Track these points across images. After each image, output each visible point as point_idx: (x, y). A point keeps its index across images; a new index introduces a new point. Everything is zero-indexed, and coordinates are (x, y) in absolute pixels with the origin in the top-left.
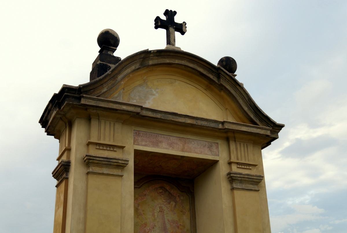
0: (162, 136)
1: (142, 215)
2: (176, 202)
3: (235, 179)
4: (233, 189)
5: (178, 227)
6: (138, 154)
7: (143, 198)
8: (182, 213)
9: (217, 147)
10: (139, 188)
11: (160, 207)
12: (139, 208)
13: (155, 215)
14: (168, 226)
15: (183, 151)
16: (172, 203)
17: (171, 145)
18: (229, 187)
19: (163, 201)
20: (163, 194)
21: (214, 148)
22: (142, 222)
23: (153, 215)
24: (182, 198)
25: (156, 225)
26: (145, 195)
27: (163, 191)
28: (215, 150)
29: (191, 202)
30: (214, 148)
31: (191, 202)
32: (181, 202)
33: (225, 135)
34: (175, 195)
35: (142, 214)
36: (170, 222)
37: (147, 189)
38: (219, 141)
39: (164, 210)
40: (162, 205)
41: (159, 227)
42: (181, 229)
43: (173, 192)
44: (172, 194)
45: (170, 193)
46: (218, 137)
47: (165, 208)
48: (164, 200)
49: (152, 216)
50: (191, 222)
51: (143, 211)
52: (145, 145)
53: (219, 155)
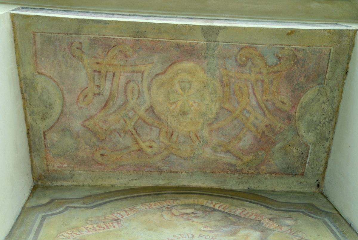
2: (264, 230)
10: (92, 207)
19: (202, 229)
24: (289, 222)
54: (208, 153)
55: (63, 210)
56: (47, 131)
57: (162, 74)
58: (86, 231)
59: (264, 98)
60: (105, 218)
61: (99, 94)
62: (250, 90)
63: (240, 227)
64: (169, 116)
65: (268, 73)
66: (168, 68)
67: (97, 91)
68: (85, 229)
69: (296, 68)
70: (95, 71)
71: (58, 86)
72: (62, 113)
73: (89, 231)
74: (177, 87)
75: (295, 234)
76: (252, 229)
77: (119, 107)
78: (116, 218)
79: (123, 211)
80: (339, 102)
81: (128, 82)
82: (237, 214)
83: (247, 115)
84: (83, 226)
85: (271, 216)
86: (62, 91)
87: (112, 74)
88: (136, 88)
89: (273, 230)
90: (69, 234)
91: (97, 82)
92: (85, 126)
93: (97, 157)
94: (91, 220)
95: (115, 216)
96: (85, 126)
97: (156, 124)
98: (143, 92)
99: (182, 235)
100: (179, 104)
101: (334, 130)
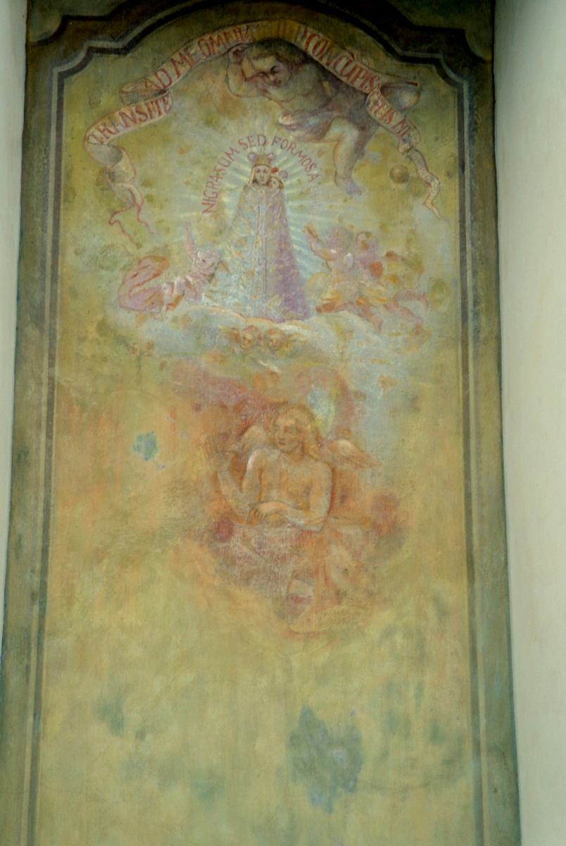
1: (139, 210)
2: (365, 127)
5: (376, 270)
7: (145, 110)
8: (402, 186)
11: (256, 161)
12: (123, 166)
13: (222, 206)
14: (308, 266)
16: (335, 131)
19: (281, 121)
20: (277, 84)
22: (139, 246)
23: (212, 204)
24: (407, 99)
25: (228, 259)
26: (162, 92)
27: (282, 66)
32: (403, 122)
34: (357, 84)
35: (139, 200)
36: (319, 241)
37: (177, 57)
39: (286, 175)
40: (269, 148)
41: (250, 274)
42: (394, 278)
43: (347, 65)
44: (344, 79)
45: (322, 70)
47: (291, 163)
48: (285, 114)
49: (205, 211)
50: (463, 235)
51: (147, 183)
55: (84, 59)
60: (146, 86)
63: (335, 114)
68: (120, 119)
73: (127, 126)
75: (406, 136)
78: (162, 87)
79: (171, 63)
82: (336, 72)
84: (117, 110)
85: (385, 79)
89: (379, 124)
90: (100, 130)
94: (126, 90)
95: (160, 80)
99: (251, 139)
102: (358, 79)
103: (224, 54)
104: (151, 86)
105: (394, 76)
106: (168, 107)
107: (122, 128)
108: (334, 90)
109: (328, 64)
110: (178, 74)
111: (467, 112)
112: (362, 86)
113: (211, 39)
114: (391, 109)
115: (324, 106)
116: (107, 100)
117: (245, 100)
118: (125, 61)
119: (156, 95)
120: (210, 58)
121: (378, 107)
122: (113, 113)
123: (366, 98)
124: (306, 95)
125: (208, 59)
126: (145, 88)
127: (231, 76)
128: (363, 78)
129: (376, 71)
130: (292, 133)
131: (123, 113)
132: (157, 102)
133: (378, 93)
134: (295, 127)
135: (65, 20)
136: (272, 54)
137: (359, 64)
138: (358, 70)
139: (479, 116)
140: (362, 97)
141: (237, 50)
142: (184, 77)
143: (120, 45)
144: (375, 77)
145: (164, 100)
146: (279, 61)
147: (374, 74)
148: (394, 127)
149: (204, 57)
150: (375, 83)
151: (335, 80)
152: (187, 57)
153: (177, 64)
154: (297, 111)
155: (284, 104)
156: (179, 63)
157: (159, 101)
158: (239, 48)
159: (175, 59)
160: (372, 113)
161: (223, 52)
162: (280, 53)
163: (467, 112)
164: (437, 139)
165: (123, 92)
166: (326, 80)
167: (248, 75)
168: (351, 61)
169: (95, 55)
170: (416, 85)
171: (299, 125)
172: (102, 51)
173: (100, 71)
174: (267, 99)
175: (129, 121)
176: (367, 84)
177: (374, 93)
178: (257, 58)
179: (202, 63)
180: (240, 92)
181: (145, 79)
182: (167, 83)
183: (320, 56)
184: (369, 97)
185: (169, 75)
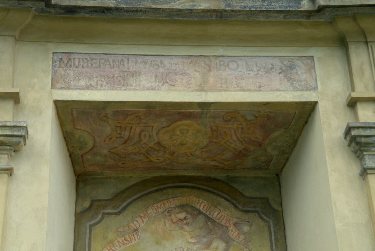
0: (140, 59)
2: (228, 241)
3: (367, 144)
4: (365, 172)
6: (67, 112)
7: (129, 239)
9: (311, 68)
10: (119, 213)
15: (202, 89)
16: (215, 244)
17: (166, 79)
18: (356, 169)
19: (190, 241)
20: (187, 224)
21: (301, 73)
24: (246, 228)
26: (136, 230)
27: (189, 216)
28: (303, 77)
29: (273, 238)
30: (301, 73)
31: (273, 238)
32: (245, 239)
33: (328, 31)
37: (142, 215)
38: (316, 52)
43: (218, 214)
45: (207, 217)
46: (314, 42)
52: (88, 88)
53: (315, 88)
54: (199, 161)
56: (84, 154)
57: (167, 127)
58: (118, 246)
59: (243, 136)
60: (129, 228)
61: (120, 137)
62: (233, 133)
63: (214, 236)
64: (171, 146)
65: (247, 124)
66: (171, 124)
67: (119, 136)
68: (117, 244)
69: (268, 121)
70: (117, 127)
71: (91, 134)
72: (94, 146)
74: (178, 133)
75: (246, 245)
76: (221, 239)
77: (135, 143)
78: (136, 228)
80: (298, 137)
81: (142, 131)
82: (214, 218)
83: (229, 144)
84: (116, 240)
85: (235, 220)
86: (93, 137)
87: (130, 128)
88: (148, 134)
89: (234, 240)
90: (108, 249)
91: (119, 132)
92: (110, 152)
93: (120, 164)
95: (135, 225)
96: (110, 152)
97: (162, 150)
98: (153, 136)
100: (179, 140)
101: (293, 150)
102: (223, 221)
103: (163, 212)
104: (131, 228)
105: (239, 219)
106: (139, 237)
107: (118, 248)
108: (213, 226)
109: (209, 214)
110: (143, 222)
111: (273, 234)
112: (225, 224)
113: (157, 206)
114: (239, 233)
115: (209, 233)
116: (111, 236)
117: (173, 232)
118: (119, 218)
119: (133, 232)
120: (157, 214)
121: (233, 233)
122: (114, 241)
123: (227, 229)
124: (201, 229)
125: (156, 215)
126: (128, 229)
127: (167, 221)
128: (225, 220)
129: (231, 217)
130: (195, 246)
131: (119, 241)
132: (134, 235)
133: (232, 226)
134: (196, 243)
135: (92, 202)
136: (184, 211)
137: (224, 214)
138: (223, 216)
139: (279, 235)
140: (226, 228)
141: (169, 210)
142: (145, 224)
143: (117, 211)
144: (231, 219)
145: (137, 234)
146: (188, 214)
147: (231, 218)
148: (241, 241)
149: (155, 214)
150: (231, 222)
151: (213, 221)
152: (147, 214)
153: (142, 218)
154: (196, 236)
155: (191, 233)
156: (143, 217)
157: (135, 235)
158: (170, 209)
159: (141, 215)
160: (231, 235)
161: (163, 211)
162: (188, 211)
163: (273, 234)
164: (260, 246)
165: (119, 232)
166: (209, 222)
167: (174, 221)
168: (220, 213)
169: (106, 216)
170: (249, 222)
171: (198, 242)
172: (109, 214)
173: (108, 223)
174: (183, 231)
175: (121, 244)
176: (228, 222)
177: (231, 227)
178: (178, 213)
179: (154, 217)
180: (171, 229)
181: (128, 225)
182: (138, 227)
183: (206, 211)
184: (229, 228)
185: (139, 223)
